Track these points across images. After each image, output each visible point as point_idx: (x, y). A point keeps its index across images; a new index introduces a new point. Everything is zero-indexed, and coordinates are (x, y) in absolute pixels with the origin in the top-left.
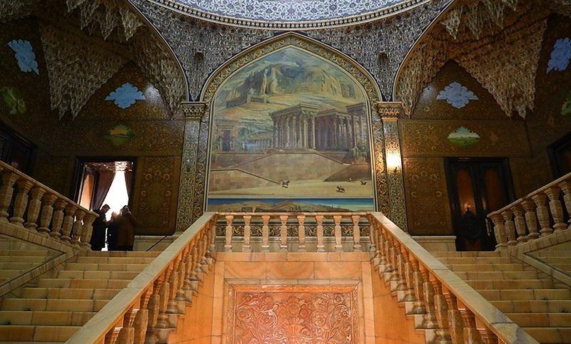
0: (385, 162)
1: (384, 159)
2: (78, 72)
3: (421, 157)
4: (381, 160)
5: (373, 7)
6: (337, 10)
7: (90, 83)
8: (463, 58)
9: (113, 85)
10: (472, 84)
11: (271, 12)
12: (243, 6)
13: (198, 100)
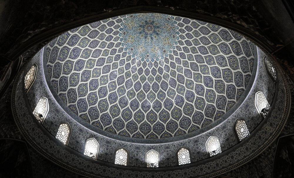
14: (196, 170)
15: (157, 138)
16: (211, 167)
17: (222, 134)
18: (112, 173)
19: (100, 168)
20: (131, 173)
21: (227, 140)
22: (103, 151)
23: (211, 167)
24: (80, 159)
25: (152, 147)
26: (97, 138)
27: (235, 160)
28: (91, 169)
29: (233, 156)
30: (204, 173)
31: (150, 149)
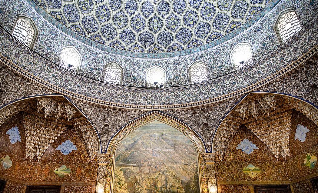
0: (208, 190)
1: (207, 188)
2: (42, 135)
3: (228, 186)
4: (206, 189)
5: (199, 98)
6: (180, 98)
7: (48, 141)
8: (250, 124)
9: (58, 142)
10: (255, 140)
11: (146, 98)
12: (130, 96)
13: (105, 153)
14: (216, 87)
15: (162, 51)
16: (236, 83)
17: (257, 38)
18: (99, 92)
19: (82, 85)
20: (126, 94)
21: (264, 44)
22: (87, 65)
23: (236, 83)
24: (54, 71)
25: (156, 63)
26: (78, 47)
27: (275, 69)
28: (70, 85)
29: (271, 64)
30: (227, 90)
31: (152, 65)
